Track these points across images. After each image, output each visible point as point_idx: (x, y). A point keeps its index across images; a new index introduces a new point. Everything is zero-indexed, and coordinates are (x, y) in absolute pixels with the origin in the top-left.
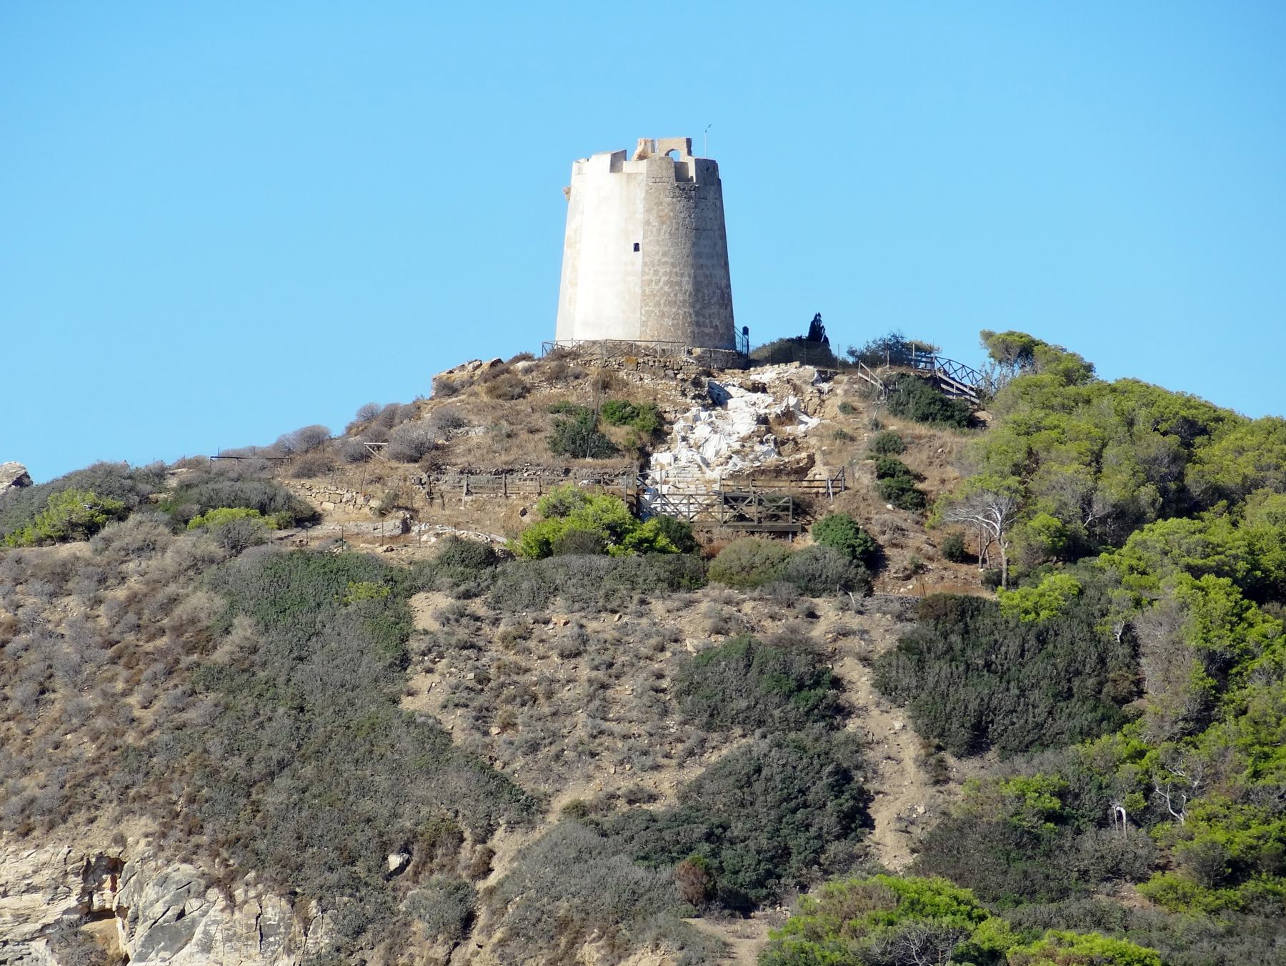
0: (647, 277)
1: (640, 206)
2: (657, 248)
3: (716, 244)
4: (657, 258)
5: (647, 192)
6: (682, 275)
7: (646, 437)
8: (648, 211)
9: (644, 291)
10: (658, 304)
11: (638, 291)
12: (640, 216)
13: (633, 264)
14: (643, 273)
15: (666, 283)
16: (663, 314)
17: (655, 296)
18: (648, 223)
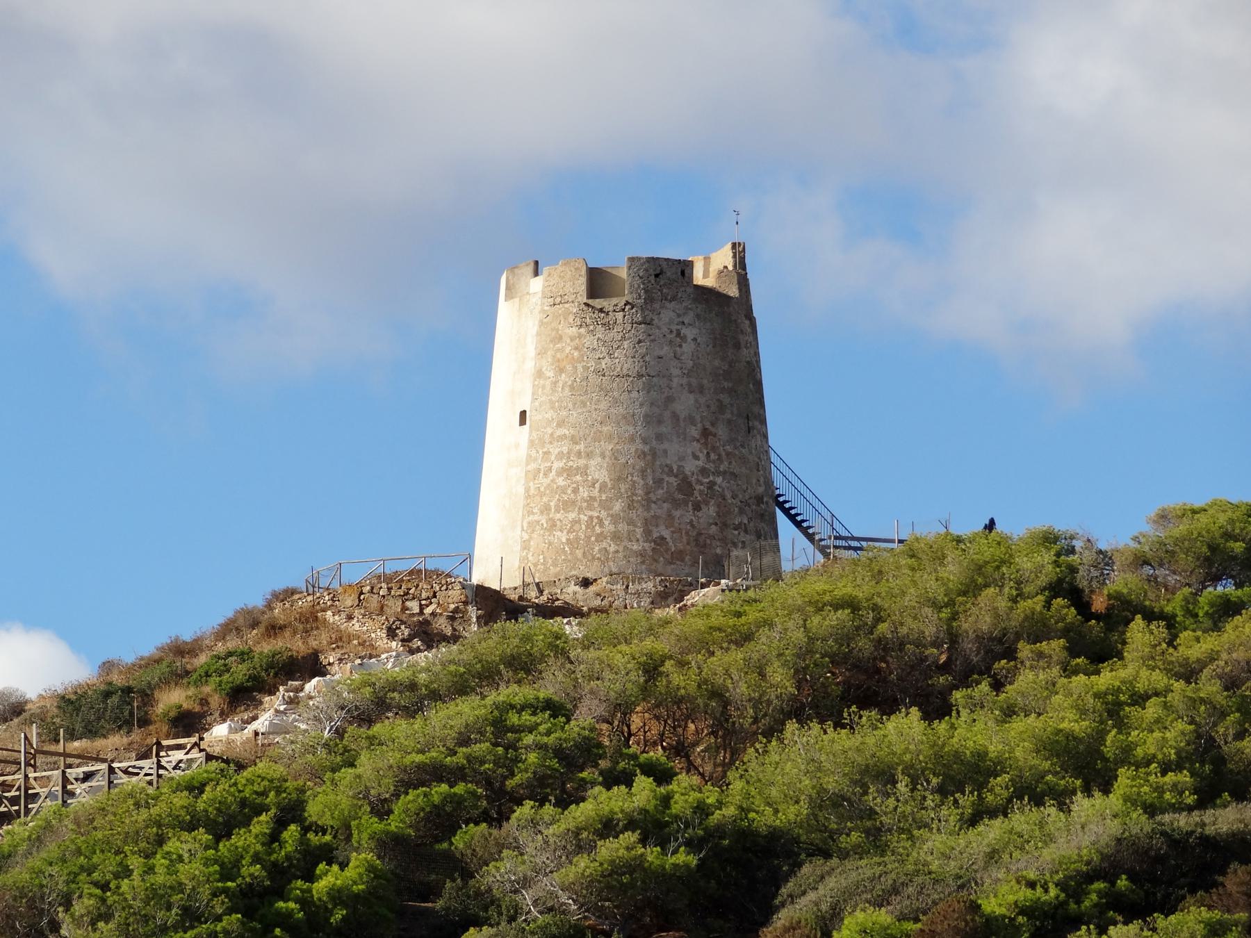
0: (533, 466)
1: (531, 350)
2: (550, 414)
3: (670, 400)
4: (549, 431)
5: (541, 323)
6: (589, 455)
7: (216, 701)
8: (541, 353)
9: (527, 490)
10: (546, 509)
11: (521, 490)
12: (530, 365)
13: (517, 446)
14: (529, 459)
15: (559, 474)
16: (553, 525)
17: (542, 495)
18: (539, 374)
